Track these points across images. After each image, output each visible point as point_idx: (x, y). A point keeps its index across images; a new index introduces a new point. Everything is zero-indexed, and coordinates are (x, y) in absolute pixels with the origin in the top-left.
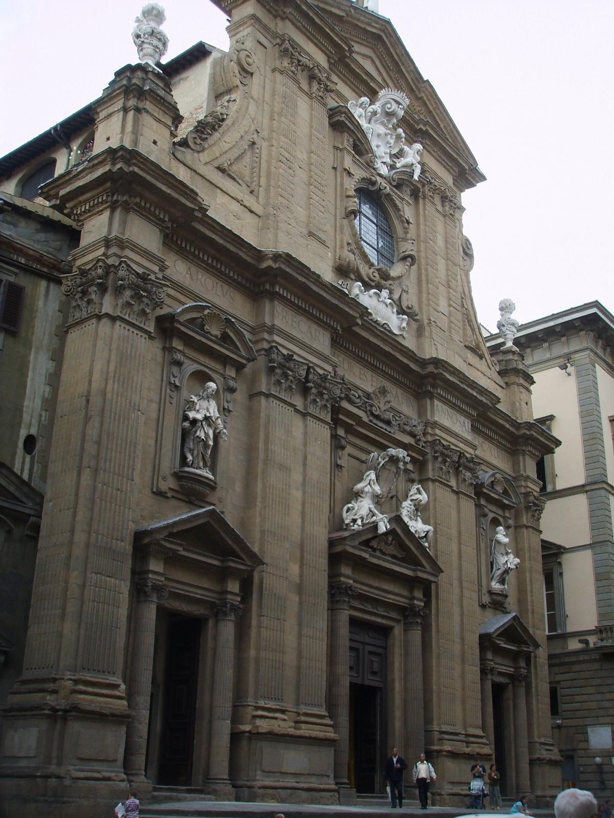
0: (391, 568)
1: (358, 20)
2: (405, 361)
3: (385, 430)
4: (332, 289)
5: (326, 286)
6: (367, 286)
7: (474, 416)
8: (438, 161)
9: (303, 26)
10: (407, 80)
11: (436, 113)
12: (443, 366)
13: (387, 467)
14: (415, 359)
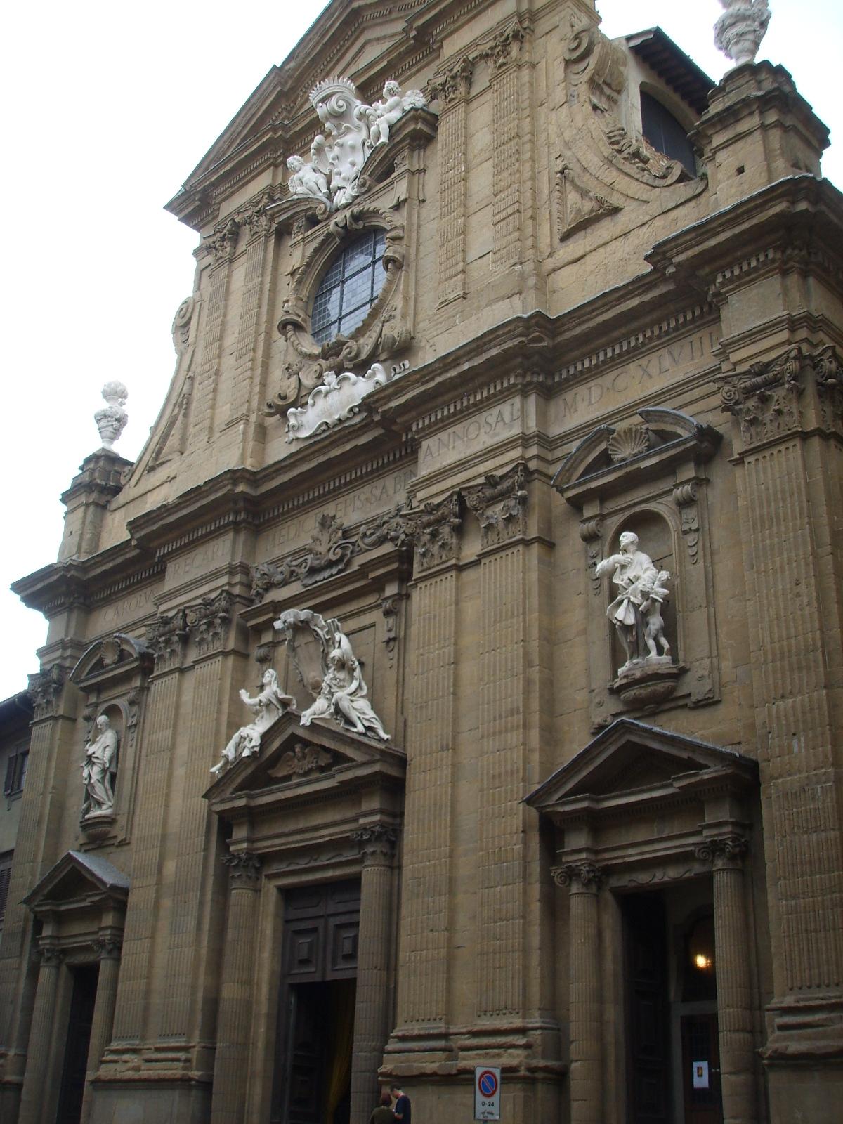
0: (296, 794)
2: (348, 447)
3: (324, 579)
4: (184, 499)
5: (180, 503)
7: (515, 385)
9: (232, 186)
13: (296, 644)
14: (359, 429)
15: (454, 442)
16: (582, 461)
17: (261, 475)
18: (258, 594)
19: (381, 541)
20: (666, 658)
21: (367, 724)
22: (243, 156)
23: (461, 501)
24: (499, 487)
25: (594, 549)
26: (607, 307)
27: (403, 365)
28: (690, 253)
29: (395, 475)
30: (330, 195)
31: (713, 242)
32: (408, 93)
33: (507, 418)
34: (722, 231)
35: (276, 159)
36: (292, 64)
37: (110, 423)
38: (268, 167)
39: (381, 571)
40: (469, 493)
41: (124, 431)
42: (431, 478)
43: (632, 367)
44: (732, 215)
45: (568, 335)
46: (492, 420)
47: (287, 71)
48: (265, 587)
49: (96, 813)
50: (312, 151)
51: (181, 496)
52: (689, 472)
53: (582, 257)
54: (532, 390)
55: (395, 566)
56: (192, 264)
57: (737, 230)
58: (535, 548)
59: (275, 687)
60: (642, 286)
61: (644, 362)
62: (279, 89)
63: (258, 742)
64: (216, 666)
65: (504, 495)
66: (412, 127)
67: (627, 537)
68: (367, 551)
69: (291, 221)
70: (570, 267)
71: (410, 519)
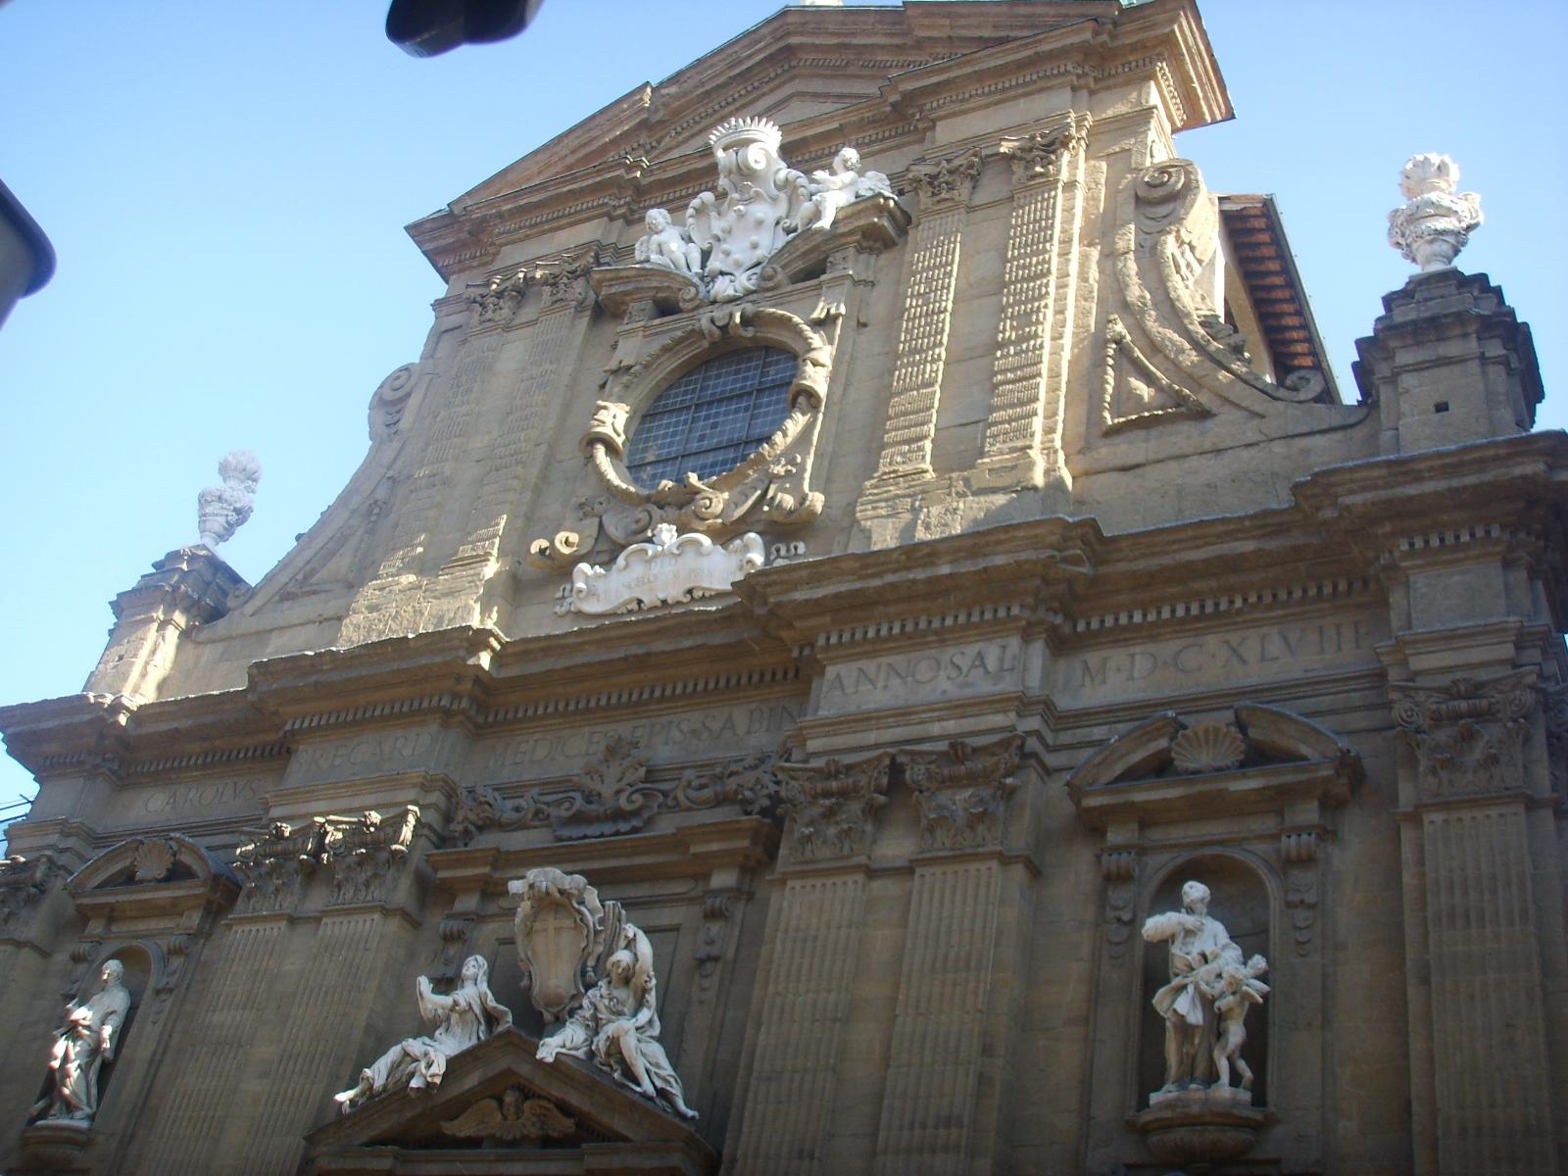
1: (702, 84)
8: (998, 102)
10: (882, 47)
11: (963, 27)
12: (769, 585)
13: (538, 926)
14: (716, 620)
15: (887, 680)
16: (1122, 756)
18: (466, 833)
19: (720, 800)
20: (1245, 1096)
21: (659, 1084)
22: (565, 189)
23: (896, 769)
24: (968, 764)
25: (1119, 896)
26: (1199, 542)
27: (796, 548)
28: (1370, 496)
29: (753, 706)
30: (709, 278)
31: (1412, 490)
32: (870, 174)
33: (992, 664)
34: (1431, 478)
35: (615, 208)
36: (673, 90)
37: (225, 512)
39: (715, 847)
40: (913, 760)
41: (240, 531)
42: (841, 723)
43: (1212, 641)
44: (1455, 459)
45: (1121, 567)
46: (964, 662)
47: (663, 96)
48: (480, 823)
49: (58, 1120)
50: (690, 211)
52: (1308, 813)
53: (1138, 466)
54: (1040, 633)
56: (429, 319)
57: (1455, 483)
58: (1019, 872)
59: (484, 987)
60: (1266, 525)
61: (1234, 638)
62: (645, 116)
63: (443, 1069)
64: (370, 926)
65: (972, 779)
67: (1195, 890)
68: (689, 809)
69: (628, 298)
70: (1115, 475)
71: (793, 778)
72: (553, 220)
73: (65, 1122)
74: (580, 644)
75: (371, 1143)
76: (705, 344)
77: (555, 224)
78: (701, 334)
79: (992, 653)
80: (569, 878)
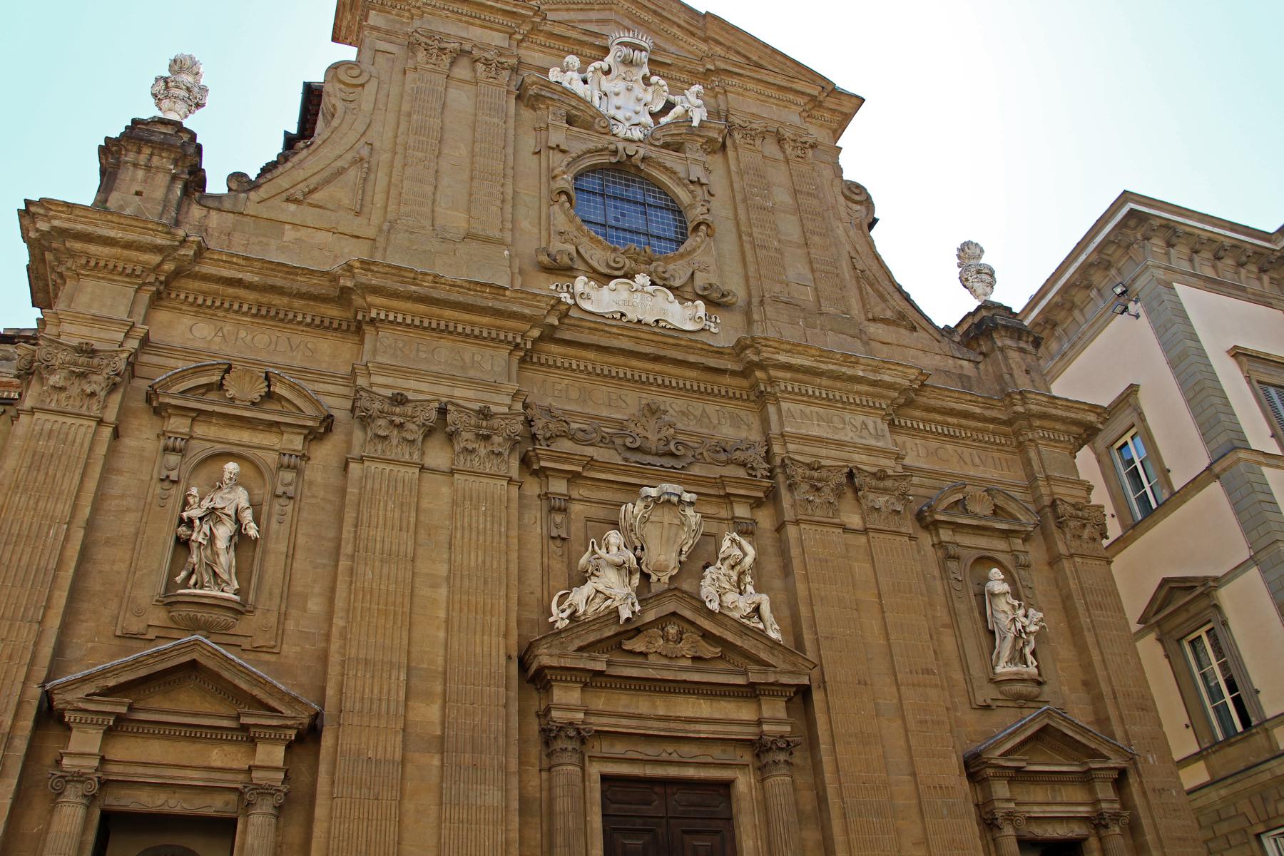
3: (662, 466)
6: (604, 278)
10: (679, 26)
17: (572, 322)
20: (1032, 670)
29: (718, 408)
38: (504, 32)
45: (924, 400)
51: (470, 282)
55: (761, 495)
65: (886, 491)
66: (716, 136)
72: (471, 16)
73: (216, 593)
74: (619, 334)
75: (581, 649)
76: (614, 160)
77: (471, 20)
78: (615, 152)
79: (870, 422)
80: (689, 495)
